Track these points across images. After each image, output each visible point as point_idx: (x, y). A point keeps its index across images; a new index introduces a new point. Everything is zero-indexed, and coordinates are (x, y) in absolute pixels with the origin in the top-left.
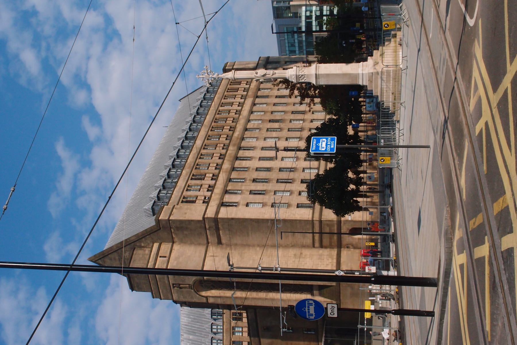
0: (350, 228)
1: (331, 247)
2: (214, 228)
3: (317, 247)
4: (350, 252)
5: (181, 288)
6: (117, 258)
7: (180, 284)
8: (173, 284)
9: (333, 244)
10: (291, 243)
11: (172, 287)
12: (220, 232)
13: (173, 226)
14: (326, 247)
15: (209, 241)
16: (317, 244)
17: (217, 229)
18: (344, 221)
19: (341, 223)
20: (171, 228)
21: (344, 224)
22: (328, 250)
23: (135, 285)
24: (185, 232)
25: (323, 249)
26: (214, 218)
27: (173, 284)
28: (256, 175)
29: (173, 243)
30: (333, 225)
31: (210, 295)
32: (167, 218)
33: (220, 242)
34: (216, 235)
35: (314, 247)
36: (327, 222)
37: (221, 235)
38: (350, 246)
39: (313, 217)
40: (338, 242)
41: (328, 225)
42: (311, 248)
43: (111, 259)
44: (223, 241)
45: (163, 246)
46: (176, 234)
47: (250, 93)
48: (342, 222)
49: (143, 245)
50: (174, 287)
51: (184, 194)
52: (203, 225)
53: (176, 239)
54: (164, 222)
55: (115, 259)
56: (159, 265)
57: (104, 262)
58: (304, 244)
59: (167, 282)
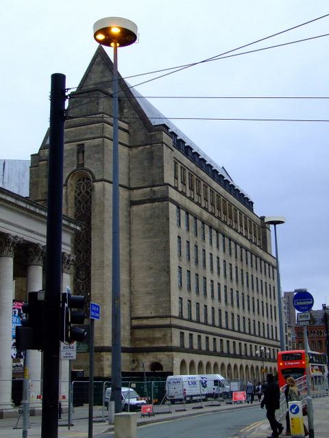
0: (162, 363)
1: (133, 339)
2: (154, 197)
3: (131, 322)
4: (128, 363)
5: (78, 153)
6: (105, 79)
7: (83, 152)
8: (83, 145)
9: (137, 342)
10: (136, 291)
11: (79, 143)
12: (149, 204)
13: (155, 147)
14: (132, 334)
15: (135, 191)
16: (135, 323)
17: (152, 201)
18: (172, 355)
19: (169, 351)
20: (151, 144)
21: (168, 356)
22: (130, 337)
23: (78, 99)
24: (146, 163)
25: (129, 331)
26: (168, 197)
27: (83, 145)
28: (200, 249)
29: (130, 147)
30: (165, 341)
31: (69, 190)
32: (164, 141)
33: (133, 203)
34: (144, 198)
35: (132, 319)
36: (169, 335)
37: (144, 205)
38: (135, 365)
39: (174, 317)
40: (141, 348)
41: (165, 335)
42: (131, 316)
43: (102, 72)
44: (135, 208)
45: (125, 134)
46: (143, 150)
47: (253, 245)
48: (170, 353)
49: (125, 111)
50: (78, 145)
51: (179, 163)
52: (158, 183)
53: (135, 151)
54: (158, 136)
55: (104, 76)
56: (108, 128)
57: (99, 64)
58: (136, 307)
59: (87, 137)
